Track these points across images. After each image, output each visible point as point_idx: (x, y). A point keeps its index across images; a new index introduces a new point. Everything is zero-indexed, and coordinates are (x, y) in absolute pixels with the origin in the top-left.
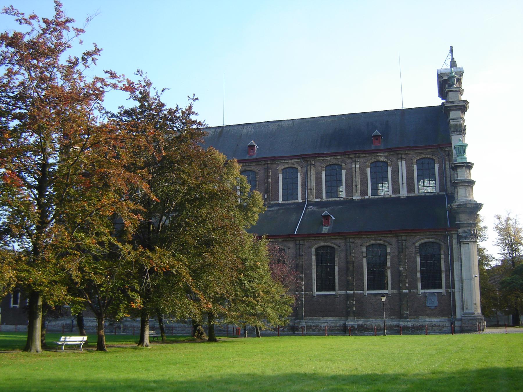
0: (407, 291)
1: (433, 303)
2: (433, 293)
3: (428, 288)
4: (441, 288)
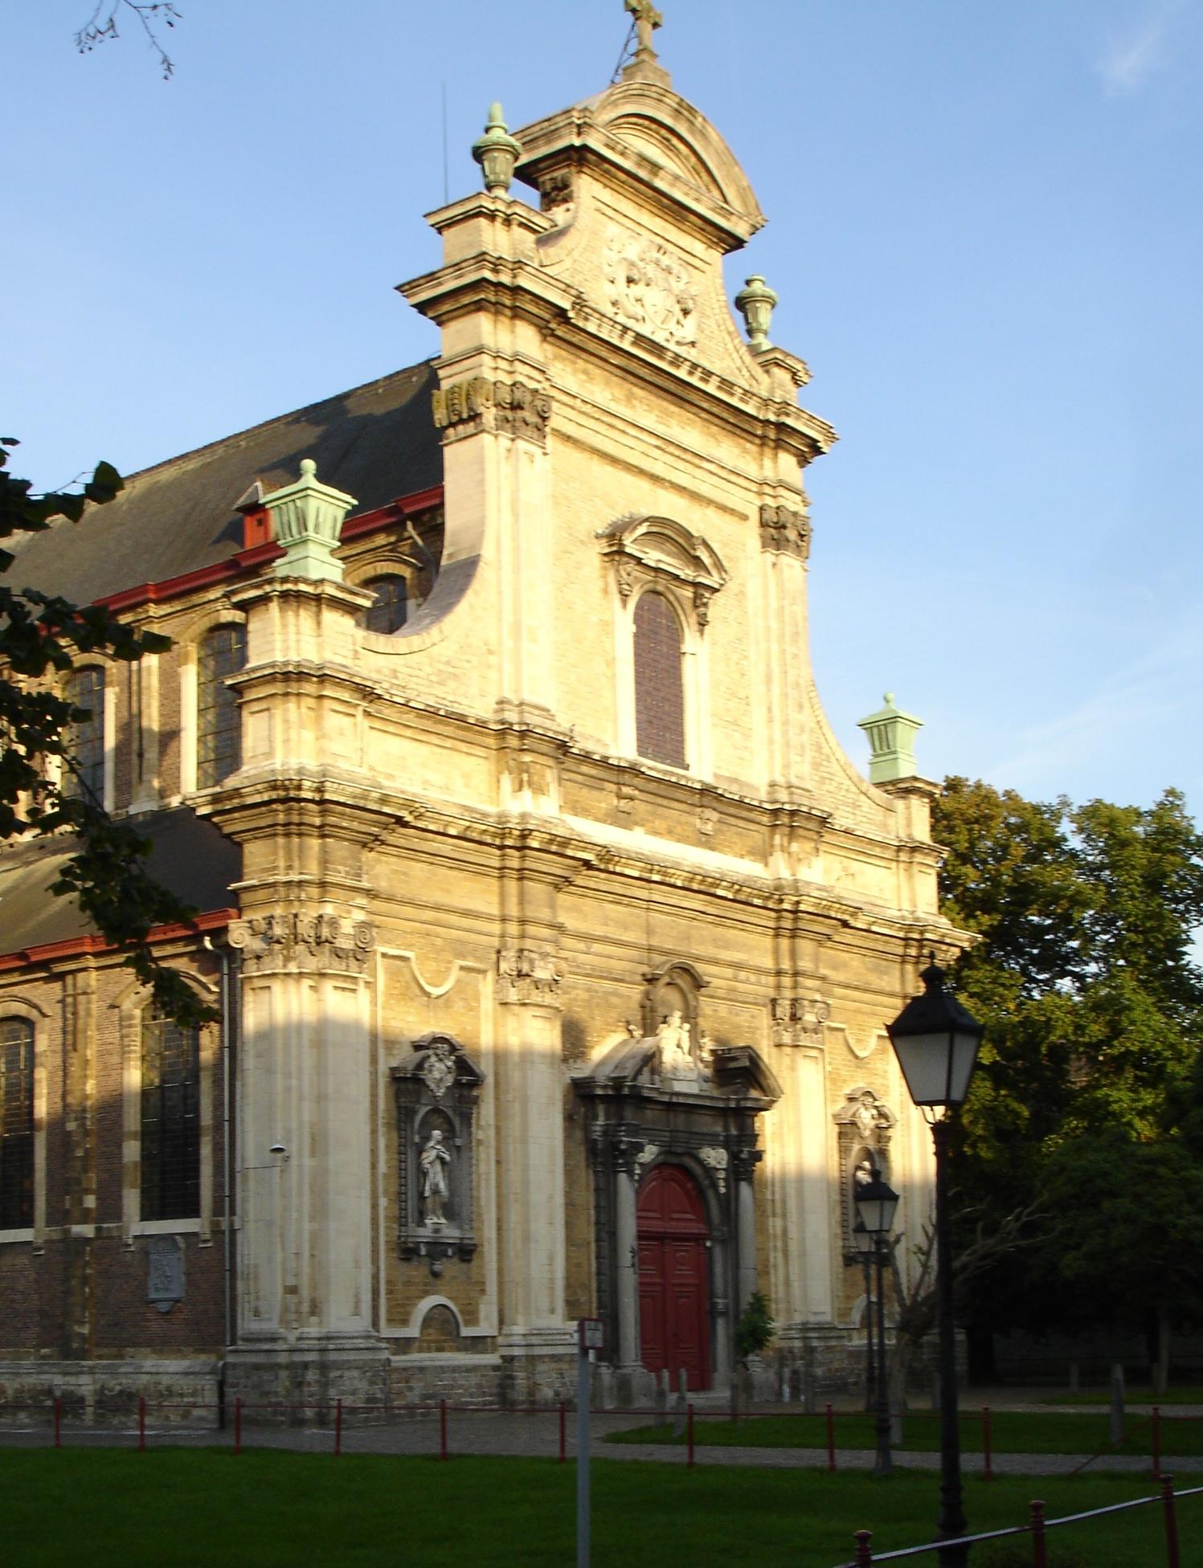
0: (87, 1230)
1: (168, 1282)
2: (170, 1237)
3: (162, 1216)
4: (193, 1211)
